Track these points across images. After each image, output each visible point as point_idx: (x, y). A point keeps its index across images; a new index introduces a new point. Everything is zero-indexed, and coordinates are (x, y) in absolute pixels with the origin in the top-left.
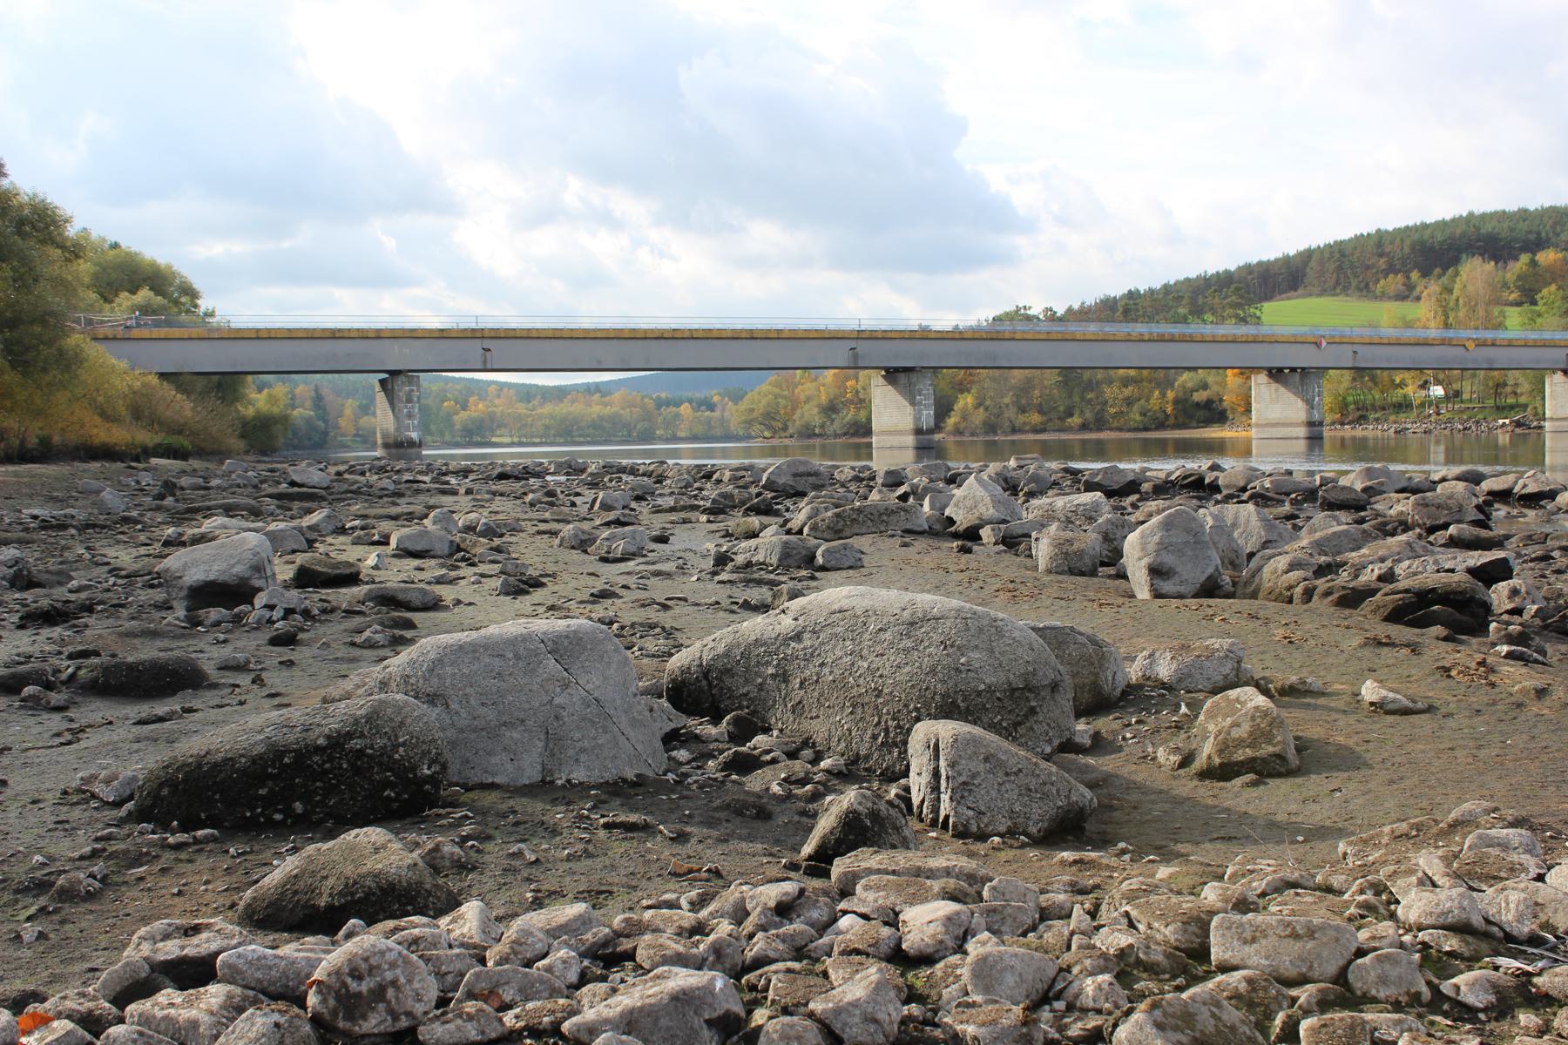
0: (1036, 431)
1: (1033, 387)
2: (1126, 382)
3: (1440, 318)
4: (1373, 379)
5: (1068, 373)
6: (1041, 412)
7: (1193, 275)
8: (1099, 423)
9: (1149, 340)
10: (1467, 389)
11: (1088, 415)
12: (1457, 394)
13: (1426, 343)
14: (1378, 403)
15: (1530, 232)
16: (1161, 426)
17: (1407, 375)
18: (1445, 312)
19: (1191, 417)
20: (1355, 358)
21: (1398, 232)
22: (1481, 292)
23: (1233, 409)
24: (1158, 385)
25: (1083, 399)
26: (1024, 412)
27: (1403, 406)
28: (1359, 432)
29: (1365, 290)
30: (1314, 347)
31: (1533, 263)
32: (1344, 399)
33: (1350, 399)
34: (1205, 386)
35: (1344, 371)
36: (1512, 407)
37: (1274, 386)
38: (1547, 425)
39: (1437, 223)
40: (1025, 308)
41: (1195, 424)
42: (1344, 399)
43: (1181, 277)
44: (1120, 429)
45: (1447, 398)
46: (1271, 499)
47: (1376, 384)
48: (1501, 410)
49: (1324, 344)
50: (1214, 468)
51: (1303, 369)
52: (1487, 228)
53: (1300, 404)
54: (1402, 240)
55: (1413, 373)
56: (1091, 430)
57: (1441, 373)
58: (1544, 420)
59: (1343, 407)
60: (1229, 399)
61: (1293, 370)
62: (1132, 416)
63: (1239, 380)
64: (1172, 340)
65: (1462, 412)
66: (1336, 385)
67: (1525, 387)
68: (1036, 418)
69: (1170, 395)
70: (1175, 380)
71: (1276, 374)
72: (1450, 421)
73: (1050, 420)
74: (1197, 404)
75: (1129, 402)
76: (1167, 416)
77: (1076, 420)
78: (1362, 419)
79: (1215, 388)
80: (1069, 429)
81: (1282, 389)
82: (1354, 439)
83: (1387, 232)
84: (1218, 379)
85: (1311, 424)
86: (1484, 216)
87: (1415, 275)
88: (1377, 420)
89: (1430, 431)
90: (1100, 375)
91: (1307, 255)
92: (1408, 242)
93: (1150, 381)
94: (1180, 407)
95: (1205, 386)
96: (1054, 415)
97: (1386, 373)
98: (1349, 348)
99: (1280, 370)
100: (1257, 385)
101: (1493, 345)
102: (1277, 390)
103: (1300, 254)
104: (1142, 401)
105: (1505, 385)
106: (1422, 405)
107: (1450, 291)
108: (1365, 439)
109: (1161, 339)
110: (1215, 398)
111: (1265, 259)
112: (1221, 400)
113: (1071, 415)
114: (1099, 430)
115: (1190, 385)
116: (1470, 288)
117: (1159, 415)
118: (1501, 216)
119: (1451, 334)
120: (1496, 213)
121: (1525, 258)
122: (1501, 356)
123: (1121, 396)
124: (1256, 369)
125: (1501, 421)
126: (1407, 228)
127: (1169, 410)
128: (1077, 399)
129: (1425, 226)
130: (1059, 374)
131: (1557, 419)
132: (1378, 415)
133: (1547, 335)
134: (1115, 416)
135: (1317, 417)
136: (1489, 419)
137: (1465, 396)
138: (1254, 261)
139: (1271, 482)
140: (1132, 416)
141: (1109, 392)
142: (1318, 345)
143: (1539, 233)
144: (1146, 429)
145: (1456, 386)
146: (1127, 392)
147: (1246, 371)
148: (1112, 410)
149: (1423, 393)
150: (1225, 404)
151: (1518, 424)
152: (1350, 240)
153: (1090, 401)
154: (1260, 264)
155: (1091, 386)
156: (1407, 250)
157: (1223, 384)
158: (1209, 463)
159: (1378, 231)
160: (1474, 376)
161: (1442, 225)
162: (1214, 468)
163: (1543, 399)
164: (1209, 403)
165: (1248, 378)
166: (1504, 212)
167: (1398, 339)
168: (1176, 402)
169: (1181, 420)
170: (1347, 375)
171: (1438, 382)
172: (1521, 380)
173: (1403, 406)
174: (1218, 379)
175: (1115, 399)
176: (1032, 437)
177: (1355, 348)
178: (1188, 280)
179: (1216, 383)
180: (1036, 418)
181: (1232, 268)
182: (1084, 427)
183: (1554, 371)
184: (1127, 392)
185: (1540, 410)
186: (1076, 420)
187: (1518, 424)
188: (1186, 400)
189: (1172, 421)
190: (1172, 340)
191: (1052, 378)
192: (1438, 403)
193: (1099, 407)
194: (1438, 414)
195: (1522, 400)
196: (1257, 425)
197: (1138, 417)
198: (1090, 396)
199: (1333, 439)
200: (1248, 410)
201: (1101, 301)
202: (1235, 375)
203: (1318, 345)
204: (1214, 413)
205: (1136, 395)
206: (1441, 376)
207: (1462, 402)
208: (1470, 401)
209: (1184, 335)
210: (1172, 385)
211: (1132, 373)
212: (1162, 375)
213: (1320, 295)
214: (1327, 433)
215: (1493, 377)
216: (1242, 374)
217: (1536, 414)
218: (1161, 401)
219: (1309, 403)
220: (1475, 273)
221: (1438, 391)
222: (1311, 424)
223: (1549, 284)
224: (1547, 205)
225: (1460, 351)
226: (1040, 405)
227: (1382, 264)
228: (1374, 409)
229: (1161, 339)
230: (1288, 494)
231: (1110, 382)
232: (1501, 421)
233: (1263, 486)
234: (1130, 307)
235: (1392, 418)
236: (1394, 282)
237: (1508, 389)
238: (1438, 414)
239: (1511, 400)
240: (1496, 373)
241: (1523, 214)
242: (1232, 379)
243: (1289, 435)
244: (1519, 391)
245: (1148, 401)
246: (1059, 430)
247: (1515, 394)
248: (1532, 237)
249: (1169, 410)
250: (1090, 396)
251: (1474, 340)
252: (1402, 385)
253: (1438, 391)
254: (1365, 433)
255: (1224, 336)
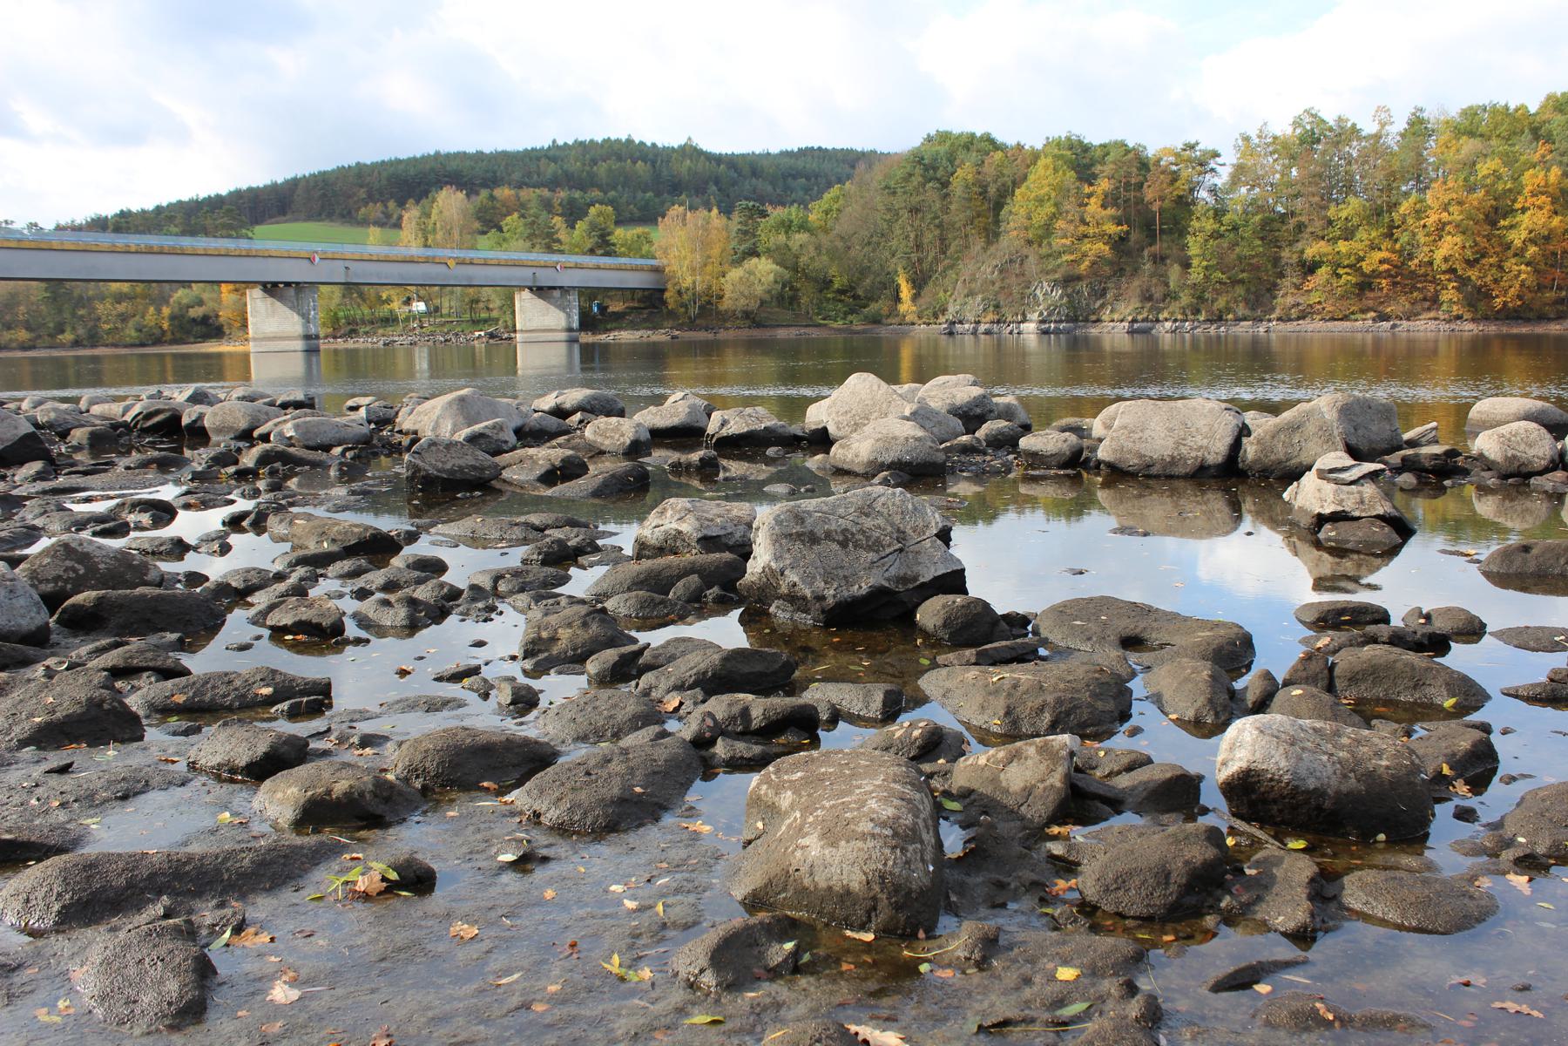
0: (24, 348)
1: (19, 304)
2: (119, 298)
3: (421, 241)
4: (361, 295)
5: (54, 283)
6: (29, 328)
7: (185, 198)
8: (93, 339)
9: (137, 252)
10: (446, 304)
11: (81, 331)
12: (437, 309)
13: (411, 261)
14: (367, 318)
15: (487, 171)
16: (158, 341)
17: (393, 292)
18: (425, 233)
19: (188, 332)
20: (347, 275)
21: (375, 166)
22: (455, 217)
23: (229, 324)
24: (153, 302)
25: (74, 315)
26: (9, 328)
27: (390, 320)
28: (351, 344)
29: (348, 216)
30: (306, 261)
31: (492, 198)
32: (336, 314)
33: (341, 314)
34: (201, 303)
35: (335, 288)
36: (485, 321)
37: (270, 300)
38: (519, 336)
39: (409, 159)
40: (6, 222)
41: (192, 340)
42: (336, 314)
43: (174, 200)
44: (115, 345)
45: (428, 313)
46: (300, 462)
47: (364, 300)
48: (476, 323)
49: (317, 259)
50: (197, 398)
51: (297, 283)
52: (453, 166)
53: (296, 318)
54: (379, 173)
55: (398, 290)
56: (84, 346)
57: (424, 289)
58: (515, 331)
59: (335, 320)
60: (224, 315)
61: (288, 284)
62: (127, 332)
63: (234, 297)
64: (161, 252)
65: (443, 325)
66: (331, 298)
67: (496, 303)
68: (23, 335)
69: (166, 311)
70: (171, 296)
71: (272, 289)
72: (432, 334)
73: (39, 337)
74: (194, 320)
75: (124, 318)
76: (164, 332)
77: (68, 337)
78: (353, 333)
79: (211, 304)
80: (62, 346)
81: (278, 304)
82: (347, 350)
83: (365, 165)
84: (214, 295)
85: (307, 337)
86: (448, 156)
87: (392, 204)
88: (366, 333)
89: (415, 343)
90: (91, 290)
91: (294, 184)
92: (385, 174)
93: (144, 297)
94: (176, 322)
95: (201, 303)
96: (43, 332)
97: (372, 290)
98: (341, 263)
99: (275, 284)
100: (252, 299)
101: (471, 263)
102: (272, 304)
103: (287, 182)
104: (137, 318)
105: (477, 301)
106: (407, 319)
107: (429, 216)
108: (356, 351)
109: (150, 251)
110: (211, 314)
111: (254, 185)
112: (217, 316)
113: (62, 332)
114: (93, 346)
115: (185, 301)
116: (446, 213)
117: (157, 331)
118: (463, 156)
119: (430, 252)
120: (459, 153)
121: (484, 193)
122: (479, 274)
123: (114, 312)
124: (250, 284)
125: (477, 334)
126: (383, 162)
127: (166, 326)
128: (67, 315)
129: (399, 162)
130: (46, 290)
131: (527, 331)
132: (367, 329)
133: (515, 256)
134: (109, 332)
135: (313, 331)
136: (466, 332)
137: (445, 311)
138: (244, 187)
139: (297, 427)
140: (127, 332)
141: (101, 308)
142: (311, 260)
143: (495, 172)
144: (143, 345)
145: (437, 302)
146: (122, 308)
147: (242, 286)
148: (107, 327)
149: (406, 309)
150: (221, 319)
151: (492, 336)
152: (333, 171)
153: (82, 316)
154: (250, 190)
155: (81, 302)
156: (384, 182)
157: (219, 301)
158: (190, 389)
159: (358, 164)
160: (452, 293)
161: (413, 161)
162: (197, 398)
163: (513, 312)
164: (205, 320)
165: (244, 294)
166: (465, 153)
167: (387, 256)
168: (173, 318)
169: (178, 335)
170: (337, 290)
171: (420, 299)
172: (493, 297)
173: (390, 320)
174: (214, 295)
175: (108, 315)
176: (20, 354)
177: (347, 264)
178: (180, 203)
179: (212, 299)
180: (23, 335)
181: (224, 193)
182: (77, 344)
183: (521, 288)
184: (122, 308)
185: (510, 323)
186: (68, 337)
187: (492, 336)
188: (183, 316)
189: (169, 336)
190: (161, 252)
191: (38, 292)
192: (420, 317)
193: (91, 324)
194: (422, 327)
195: (495, 314)
196: (255, 339)
197: (134, 333)
198: (81, 312)
199: (328, 351)
200: (245, 325)
201: (93, 220)
202: (230, 292)
203: (311, 260)
204: (211, 328)
205: (130, 311)
206: (422, 292)
207: (441, 316)
208: (449, 315)
209: (174, 248)
210: (167, 303)
211: (125, 287)
212: (155, 290)
213: (309, 218)
214: (324, 345)
215: (468, 294)
216: (236, 290)
217: (506, 327)
218: (158, 317)
219: (305, 317)
220: (450, 203)
221: (420, 307)
222: (307, 337)
223: (509, 214)
224: (500, 149)
225: (443, 268)
226: (27, 321)
227: (362, 193)
228: (363, 322)
229: (150, 251)
230: (327, 448)
231: (102, 298)
232: (477, 334)
233: (281, 434)
234: (124, 222)
235: (381, 331)
236: (375, 210)
237: (481, 305)
238: (422, 327)
239: (484, 315)
240: (471, 290)
241: (479, 156)
242: (227, 295)
243: (287, 348)
244: (491, 306)
245: (143, 317)
246: (50, 347)
247: (488, 309)
248: (489, 175)
249: (166, 326)
250: (81, 312)
251: (454, 258)
252: (388, 301)
253: (420, 307)
254: (356, 346)
255: (216, 249)
